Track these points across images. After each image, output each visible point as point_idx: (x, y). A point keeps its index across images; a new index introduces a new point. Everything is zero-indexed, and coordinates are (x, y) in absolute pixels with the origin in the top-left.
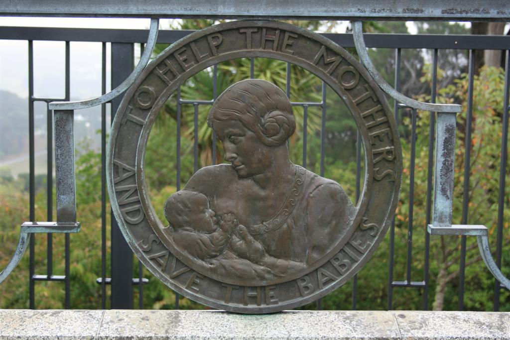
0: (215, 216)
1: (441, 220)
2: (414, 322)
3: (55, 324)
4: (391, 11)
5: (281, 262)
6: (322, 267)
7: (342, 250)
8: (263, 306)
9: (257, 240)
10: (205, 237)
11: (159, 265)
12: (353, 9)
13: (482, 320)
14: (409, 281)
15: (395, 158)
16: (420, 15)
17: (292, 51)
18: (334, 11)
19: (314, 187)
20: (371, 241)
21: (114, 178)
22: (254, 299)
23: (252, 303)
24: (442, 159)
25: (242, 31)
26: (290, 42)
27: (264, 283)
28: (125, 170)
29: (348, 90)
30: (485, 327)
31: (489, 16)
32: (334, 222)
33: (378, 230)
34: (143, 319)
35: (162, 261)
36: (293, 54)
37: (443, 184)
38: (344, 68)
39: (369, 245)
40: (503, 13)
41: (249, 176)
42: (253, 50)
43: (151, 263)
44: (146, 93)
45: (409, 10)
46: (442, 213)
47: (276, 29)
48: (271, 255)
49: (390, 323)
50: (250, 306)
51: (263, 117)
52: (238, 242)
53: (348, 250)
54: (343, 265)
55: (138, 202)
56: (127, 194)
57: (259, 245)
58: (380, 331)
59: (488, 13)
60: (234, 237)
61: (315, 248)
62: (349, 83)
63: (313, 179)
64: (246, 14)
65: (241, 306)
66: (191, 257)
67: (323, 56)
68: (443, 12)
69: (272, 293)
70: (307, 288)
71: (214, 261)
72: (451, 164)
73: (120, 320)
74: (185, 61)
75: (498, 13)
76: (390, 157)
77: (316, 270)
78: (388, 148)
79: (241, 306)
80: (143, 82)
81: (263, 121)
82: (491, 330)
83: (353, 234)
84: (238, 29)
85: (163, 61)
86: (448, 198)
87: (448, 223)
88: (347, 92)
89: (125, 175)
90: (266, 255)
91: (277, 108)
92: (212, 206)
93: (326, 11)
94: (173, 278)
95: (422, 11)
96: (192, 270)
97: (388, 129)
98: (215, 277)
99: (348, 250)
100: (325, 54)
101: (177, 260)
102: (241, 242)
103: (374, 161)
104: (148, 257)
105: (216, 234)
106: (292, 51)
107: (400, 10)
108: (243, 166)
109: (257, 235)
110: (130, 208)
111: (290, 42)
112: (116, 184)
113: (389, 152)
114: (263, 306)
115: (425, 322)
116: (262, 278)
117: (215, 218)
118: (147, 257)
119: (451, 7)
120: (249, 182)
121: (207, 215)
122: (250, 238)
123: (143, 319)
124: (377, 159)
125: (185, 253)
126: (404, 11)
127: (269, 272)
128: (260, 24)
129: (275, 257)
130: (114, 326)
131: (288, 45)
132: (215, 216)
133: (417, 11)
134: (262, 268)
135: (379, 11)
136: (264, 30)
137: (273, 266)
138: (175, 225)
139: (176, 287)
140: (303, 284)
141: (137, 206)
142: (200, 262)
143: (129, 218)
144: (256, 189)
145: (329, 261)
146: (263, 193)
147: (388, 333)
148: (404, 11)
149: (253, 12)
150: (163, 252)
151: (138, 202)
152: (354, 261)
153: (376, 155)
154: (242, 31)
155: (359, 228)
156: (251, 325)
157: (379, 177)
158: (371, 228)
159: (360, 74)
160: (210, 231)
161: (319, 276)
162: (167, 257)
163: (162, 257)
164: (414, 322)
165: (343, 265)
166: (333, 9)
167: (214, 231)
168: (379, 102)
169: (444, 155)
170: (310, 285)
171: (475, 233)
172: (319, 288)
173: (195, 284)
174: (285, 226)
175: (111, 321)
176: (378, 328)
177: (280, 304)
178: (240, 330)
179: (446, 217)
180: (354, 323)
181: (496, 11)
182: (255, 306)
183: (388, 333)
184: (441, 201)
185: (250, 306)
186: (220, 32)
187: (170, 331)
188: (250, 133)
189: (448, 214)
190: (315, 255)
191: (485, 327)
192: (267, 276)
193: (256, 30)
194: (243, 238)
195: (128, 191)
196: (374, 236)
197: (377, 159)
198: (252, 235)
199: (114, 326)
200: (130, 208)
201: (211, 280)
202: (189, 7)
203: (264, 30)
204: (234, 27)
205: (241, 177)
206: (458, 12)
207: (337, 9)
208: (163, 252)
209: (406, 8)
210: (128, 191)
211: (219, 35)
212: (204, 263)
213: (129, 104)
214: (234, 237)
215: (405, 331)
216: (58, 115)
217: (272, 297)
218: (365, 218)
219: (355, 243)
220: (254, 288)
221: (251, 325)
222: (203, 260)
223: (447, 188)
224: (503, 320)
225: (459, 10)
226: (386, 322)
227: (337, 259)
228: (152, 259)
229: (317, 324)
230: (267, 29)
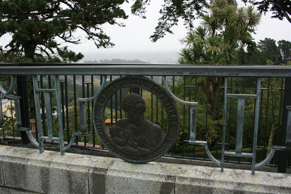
0: (123, 134)
1: (192, 140)
2: (183, 171)
3: (80, 161)
4: (173, 73)
5: (142, 149)
6: (155, 151)
7: (160, 147)
8: (138, 161)
9: (136, 142)
10: (121, 140)
11: (108, 147)
12: (161, 73)
13: (205, 171)
14: (183, 157)
15: (176, 119)
16: (182, 74)
17: (143, 85)
18: (155, 73)
19: (152, 127)
20: (170, 145)
21: (95, 121)
22: (135, 159)
23: (135, 160)
24: (192, 120)
25: (129, 79)
26: (143, 82)
27: (138, 155)
28: (98, 119)
29: (161, 98)
30: (204, 174)
31: (205, 75)
32: (158, 138)
33: (172, 141)
34: (104, 162)
35: (109, 146)
36: (144, 86)
37: (192, 128)
38: (160, 91)
39: (169, 146)
40: (210, 74)
41: (132, 123)
42: (132, 85)
43: (106, 146)
44: (103, 97)
45: (179, 73)
46: (192, 137)
47: (138, 79)
48: (140, 147)
49: (175, 170)
50: (134, 161)
51: (136, 105)
52: (130, 142)
53: (162, 147)
54: (161, 151)
55: (101, 128)
56: (99, 126)
57: (136, 143)
58: (170, 173)
59: (205, 74)
60: (129, 140)
61: (152, 145)
62: (161, 95)
63: (151, 124)
64: (129, 74)
65: (132, 161)
66: (117, 145)
67: (153, 87)
68: (190, 74)
69: (140, 158)
70: (151, 157)
71: (123, 147)
72: (195, 122)
73: (98, 162)
74: (113, 88)
75: (208, 74)
76: (175, 119)
77: (153, 152)
78: (174, 116)
79: (132, 161)
80: (101, 94)
81: (136, 106)
82: (206, 176)
83: (164, 142)
84: (127, 79)
85: (107, 88)
86: (194, 133)
87: (194, 141)
88: (161, 98)
89: (98, 120)
90: (138, 146)
91: (140, 103)
92: (123, 131)
93: (153, 73)
94: (112, 151)
95: (183, 73)
96: (117, 149)
97: (174, 110)
98: (123, 152)
99: (162, 147)
100: (154, 86)
101: (113, 146)
102: (131, 142)
103: (170, 120)
104: (106, 144)
105: (123, 139)
106: (143, 85)
107: (176, 73)
108: (130, 120)
109: (135, 140)
110: (100, 130)
111: (143, 82)
112: (96, 123)
113: (175, 117)
114: (138, 161)
115: (186, 171)
116: (137, 153)
117: (123, 135)
118: (105, 144)
119: (192, 72)
120: (133, 124)
121: (121, 133)
122: (133, 141)
123: (104, 162)
124: (171, 119)
125: (115, 144)
126: (177, 73)
127: (139, 152)
128: (134, 77)
129: (141, 147)
130: (95, 163)
131: (142, 84)
132: (123, 134)
133: (181, 73)
134: (137, 150)
135: (169, 73)
136: (135, 79)
137: (140, 150)
138: (112, 136)
139: (113, 153)
140: (150, 156)
141: (101, 130)
142: (119, 147)
143: (100, 133)
144: (135, 126)
145: (157, 150)
146: (137, 128)
147: (172, 174)
148: (177, 73)
149: (131, 74)
150: (109, 143)
151: (101, 128)
152: (165, 150)
153: (170, 118)
154: (129, 79)
155: (166, 140)
156: (133, 167)
157: (172, 125)
158: (170, 141)
159: (165, 93)
160: (122, 138)
161: (154, 154)
162: (110, 145)
163: (109, 144)
164: (183, 171)
165: (161, 151)
166: (155, 73)
167: (123, 138)
168: (171, 101)
169: (193, 119)
170: (151, 156)
171: (202, 144)
172: (154, 158)
173: (118, 153)
174: (143, 138)
175: (95, 162)
176: (170, 172)
177: (143, 161)
178: (129, 168)
179: (193, 139)
180: (164, 169)
181: (207, 73)
182: (136, 161)
183: (172, 174)
184: (192, 133)
185: (134, 161)
186: (122, 79)
187: (109, 167)
188: (132, 110)
189: (194, 138)
190: (152, 148)
191: (204, 174)
192: (138, 153)
193: (132, 79)
194: (131, 141)
195: (99, 125)
196: (171, 143)
197: (171, 119)
198: (134, 140)
199: (95, 163)
200: (100, 130)
201: (123, 153)
202: (113, 72)
203: (135, 79)
204: (126, 78)
205: (130, 123)
206: (194, 74)
207: (156, 73)
208: (109, 143)
209: (177, 72)
210: (99, 125)
211: (122, 80)
212: (120, 147)
213: (98, 100)
214: (129, 140)
215: (178, 174)
216: (80, 103)
217: (141, 159)
218: (168, 137)
219: (165, 145)
220: (135, 156)
221: (133, 167)
222: (120, 146)
223: (194, 129)
224: (212, 172)
225: (195, 73)
226: (174, 170)
227: (159, 149)
228: (106, 145)
229: (152, 169)
230: (136, 78)
